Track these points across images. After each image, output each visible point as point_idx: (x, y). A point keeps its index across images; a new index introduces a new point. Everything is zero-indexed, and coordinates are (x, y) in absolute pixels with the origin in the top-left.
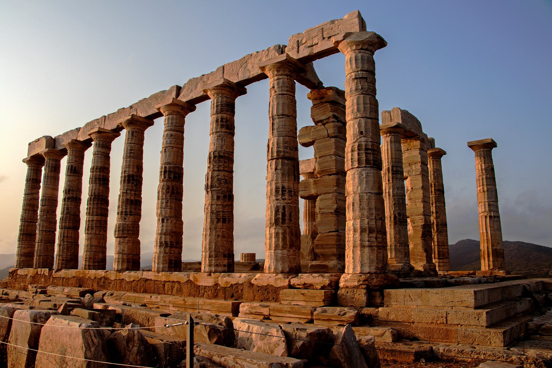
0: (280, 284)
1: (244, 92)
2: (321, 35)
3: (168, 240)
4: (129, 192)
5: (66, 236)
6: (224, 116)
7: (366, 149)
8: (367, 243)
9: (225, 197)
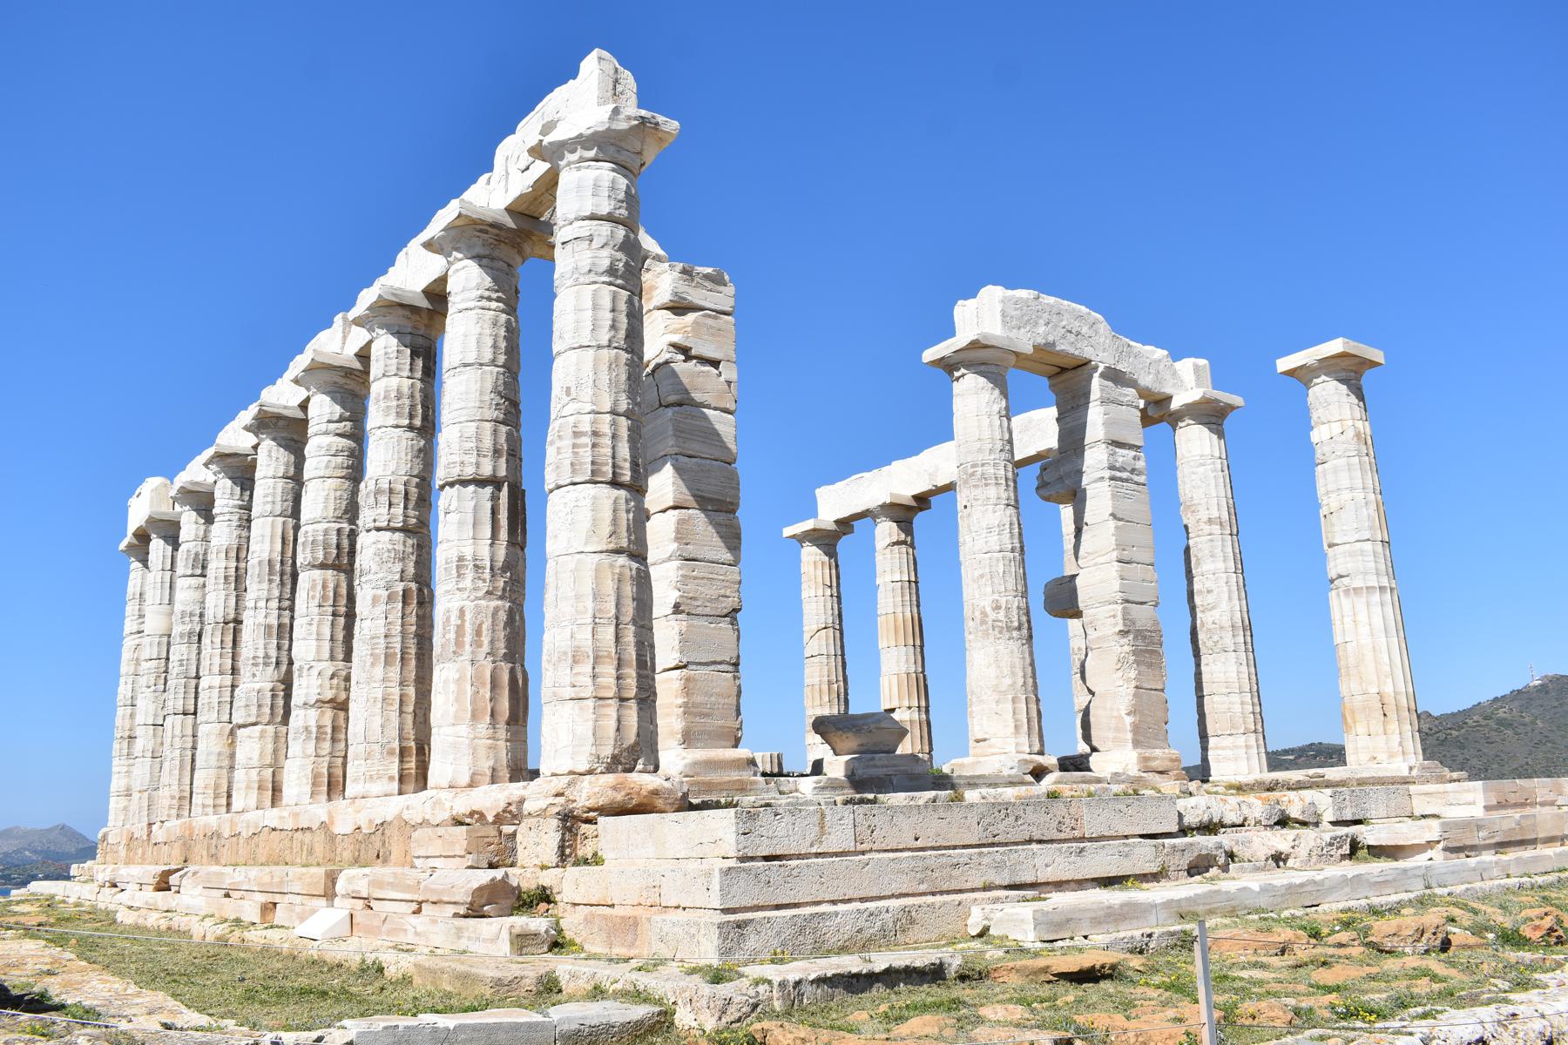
4: (262, 604)
5: (178, 732)
7: (576, 434)
9: (390, 599)
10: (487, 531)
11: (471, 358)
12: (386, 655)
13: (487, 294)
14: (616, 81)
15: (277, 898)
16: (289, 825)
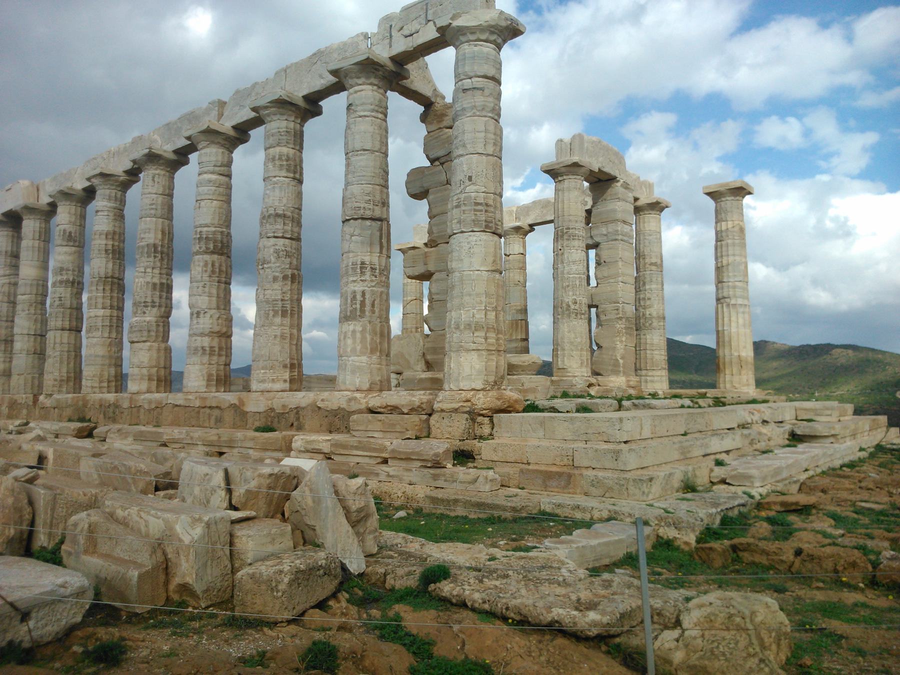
0: (354, 407)
1: (318, 112)
2: (423, 16)
3: (206, 344)
4: (149, 270)
5: (58, 340)
9: (285, 278)
10: (378, 250)
11: (368, 146)
12: (282, 311)
13: (376, 108)
15: (224, 450)
16: (198, 403)
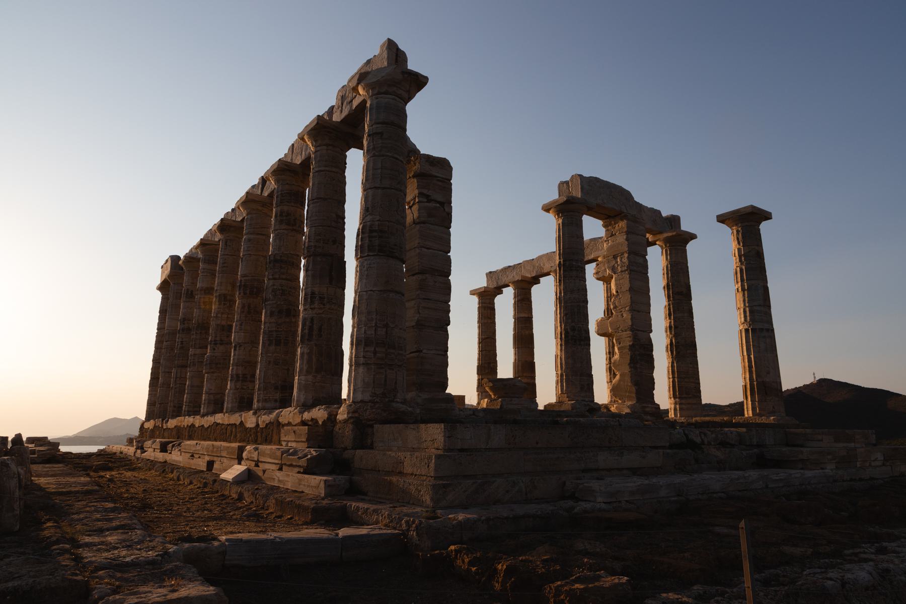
3: (240, 372)
6: (285, 208)
7: (371, 231)
8: (362, 360)
14: (397, 55)
